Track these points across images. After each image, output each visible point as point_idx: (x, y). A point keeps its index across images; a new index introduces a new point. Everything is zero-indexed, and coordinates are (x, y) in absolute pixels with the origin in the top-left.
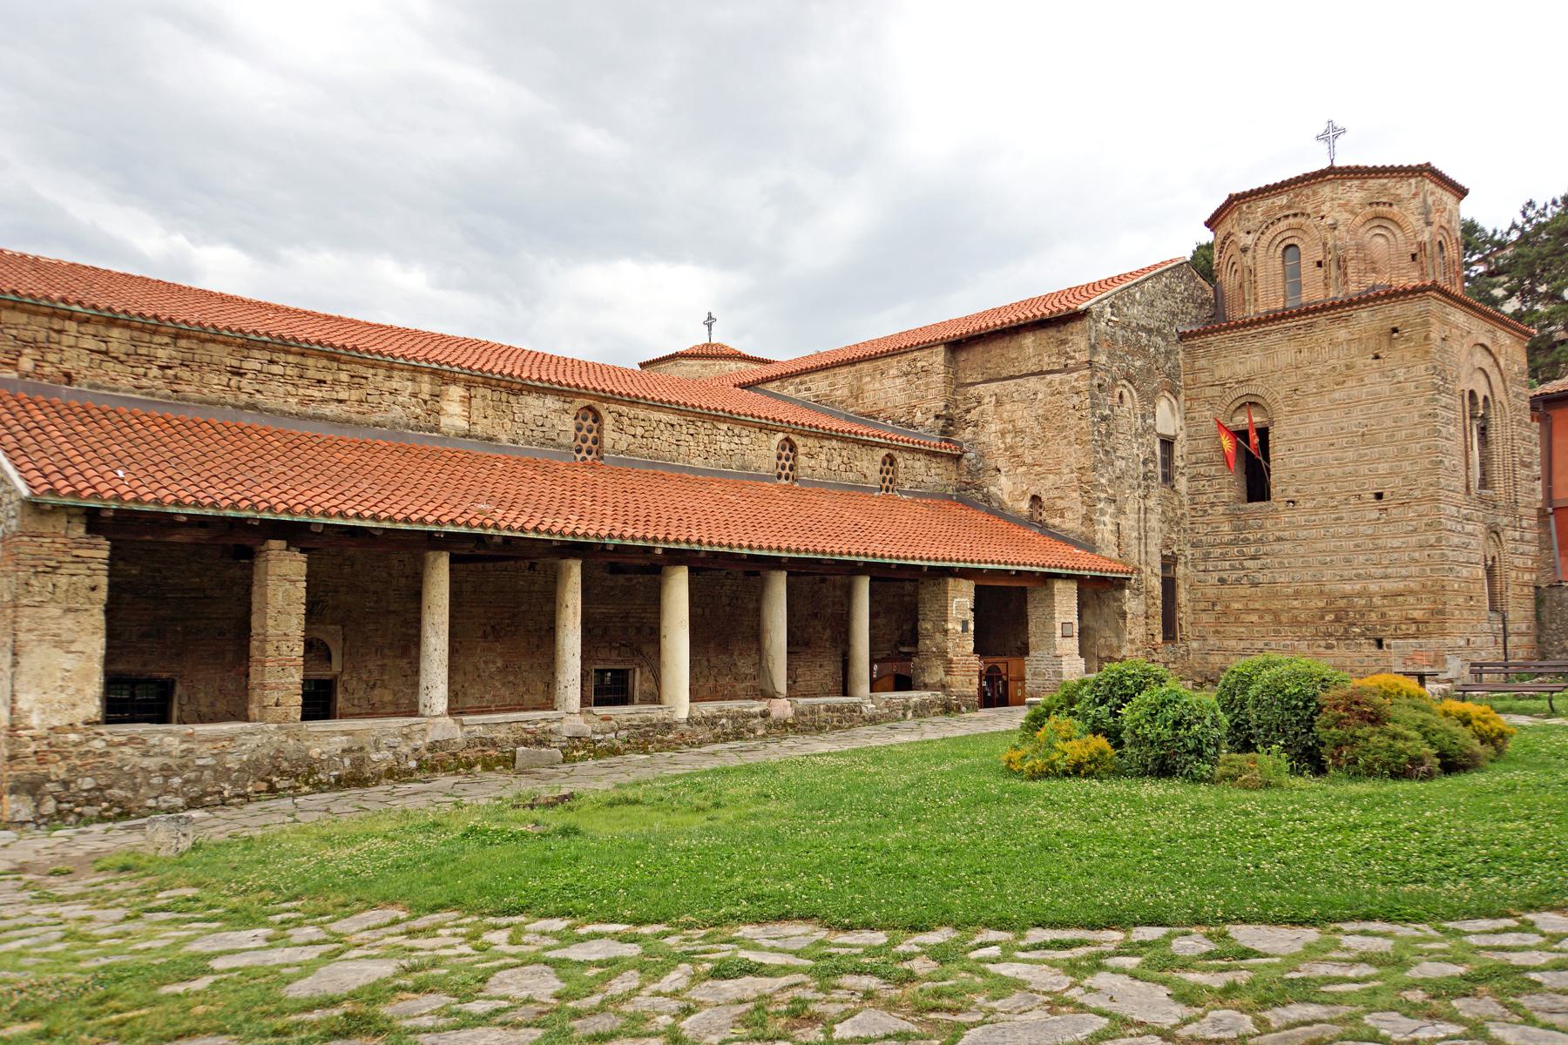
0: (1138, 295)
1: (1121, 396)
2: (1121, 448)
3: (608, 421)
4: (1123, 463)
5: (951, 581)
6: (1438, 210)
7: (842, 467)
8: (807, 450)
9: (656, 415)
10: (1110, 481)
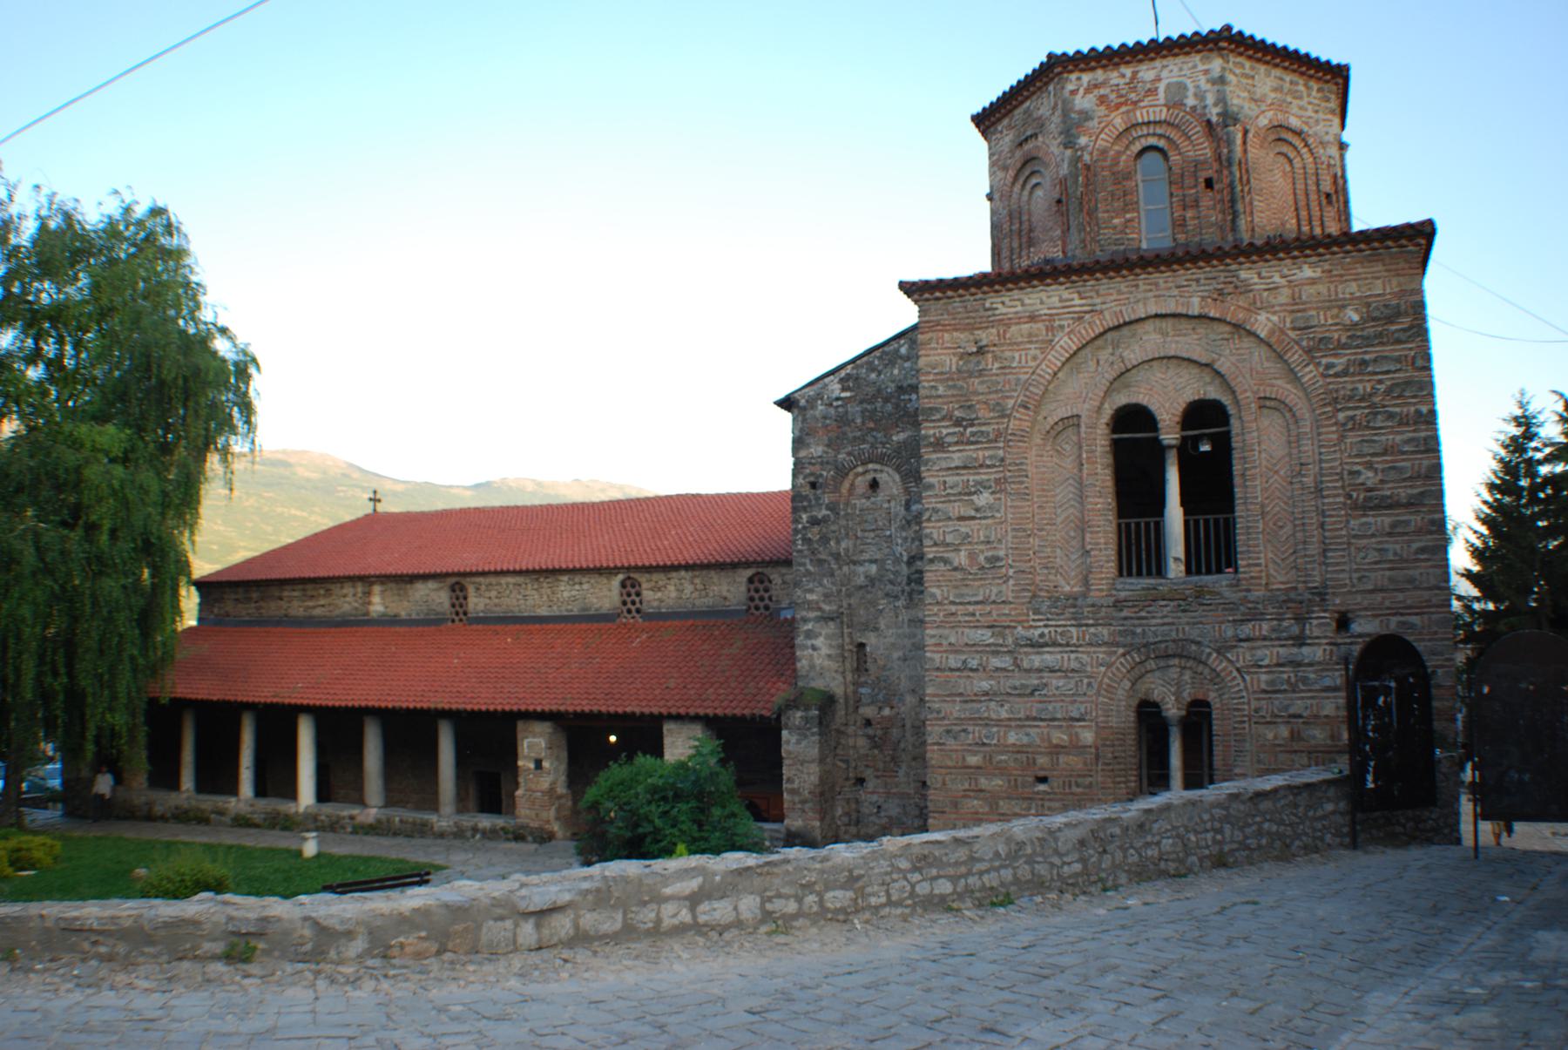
0: (903, 350)
1: (874, 485)
2: (874, 548)
3: (471, 590)
4: (873, 569)
5: (520, 725)
6: (1118, 106)
7: (696, 594)
8: (653, 584)
9: (504, 580)
10: (826, 596)
